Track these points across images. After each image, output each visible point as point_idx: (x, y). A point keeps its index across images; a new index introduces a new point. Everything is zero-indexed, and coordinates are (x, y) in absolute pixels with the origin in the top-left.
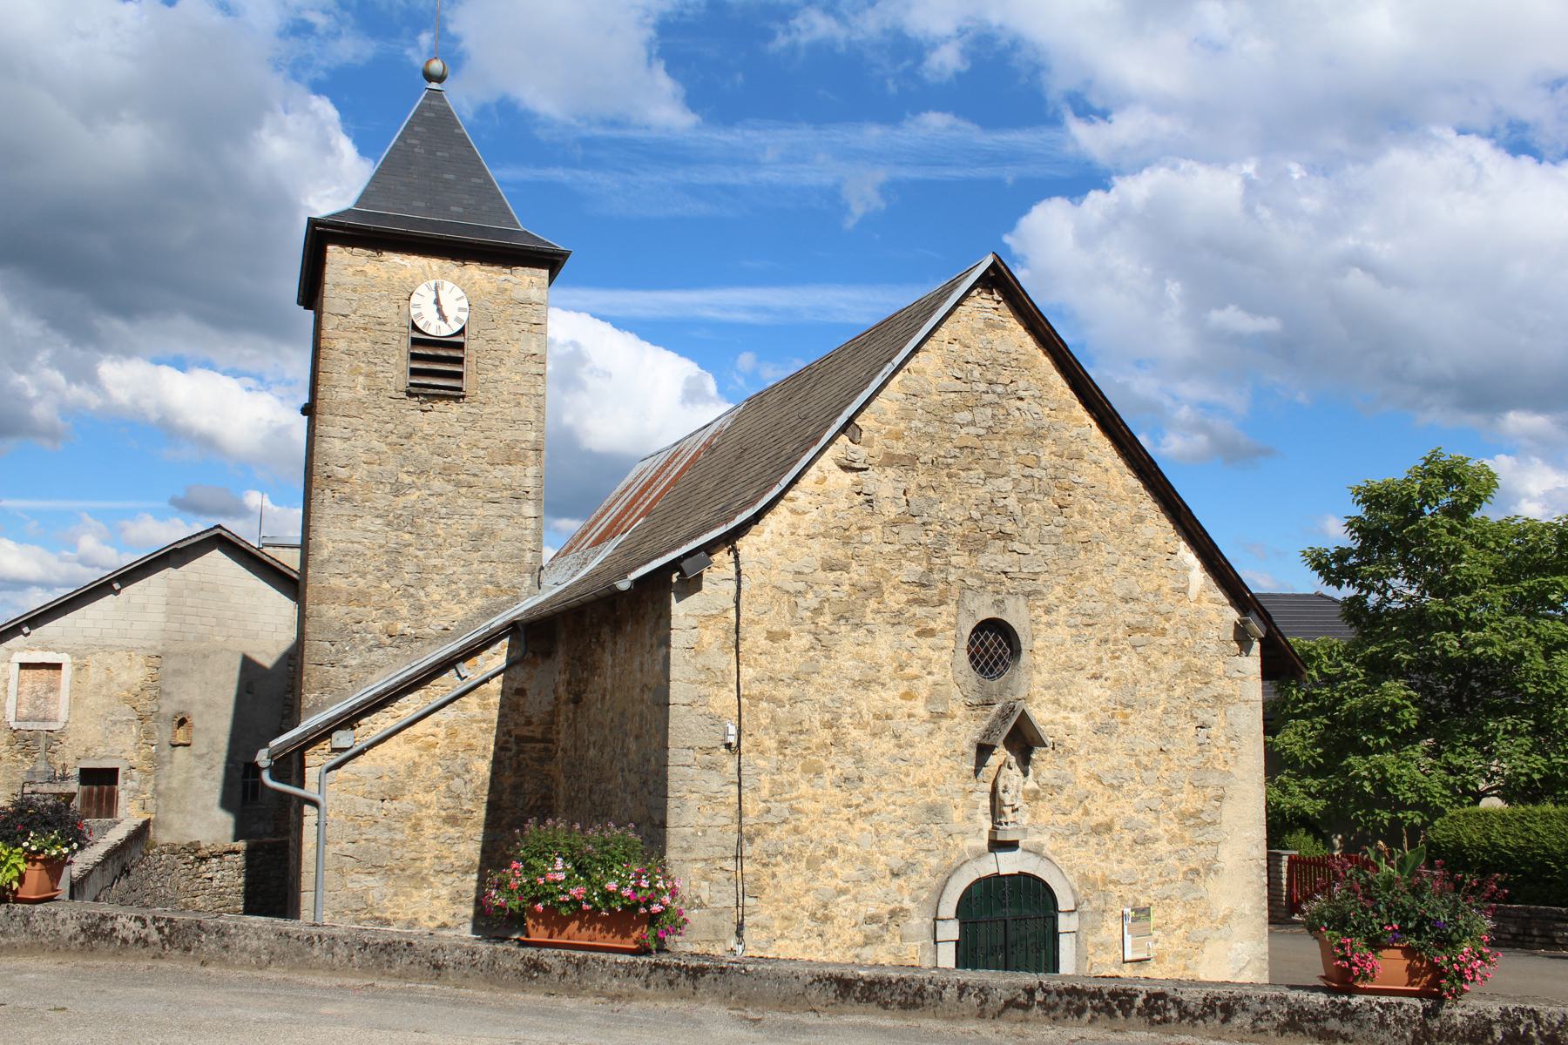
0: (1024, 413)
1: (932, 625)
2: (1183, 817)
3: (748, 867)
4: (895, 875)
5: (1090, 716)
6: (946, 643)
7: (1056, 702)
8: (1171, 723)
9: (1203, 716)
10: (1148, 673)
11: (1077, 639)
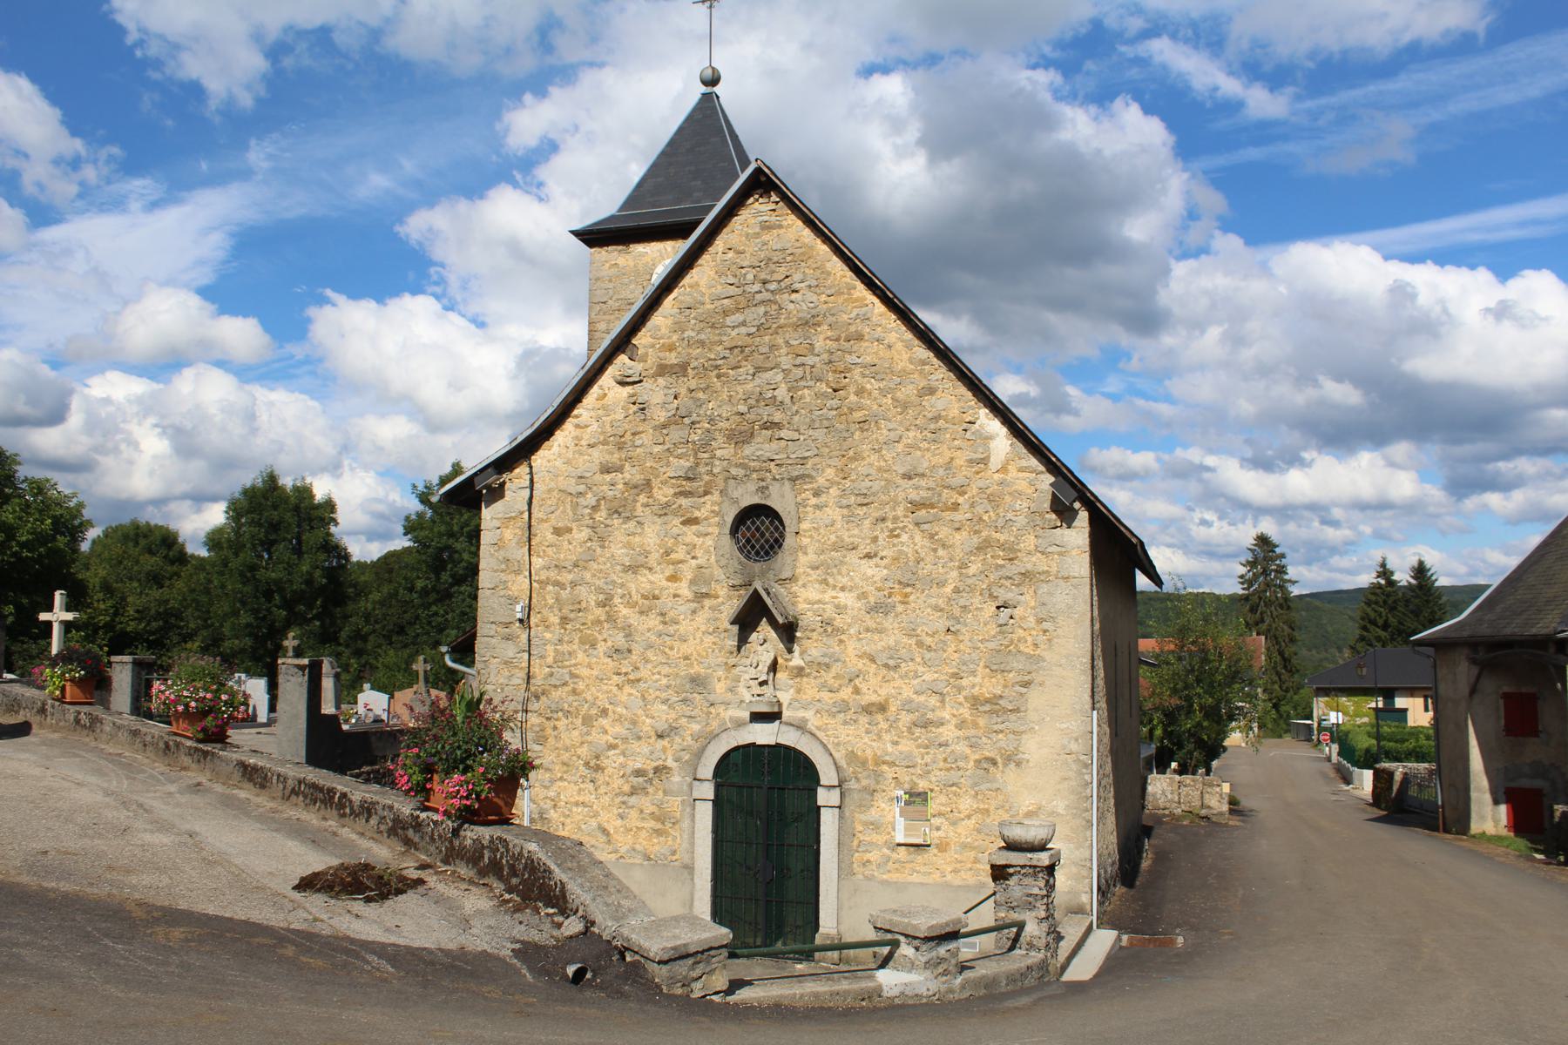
0: (797, 305)
1: (697, 514)
2: (975, 702)
3: (534, 719)
4: (660, 736)
5: (863, 596)
6: (710, 530)
7: (825, 582)
8: (962, 602)
9: (1004, 595)
10: (935, 550)
11: (849, 519)
